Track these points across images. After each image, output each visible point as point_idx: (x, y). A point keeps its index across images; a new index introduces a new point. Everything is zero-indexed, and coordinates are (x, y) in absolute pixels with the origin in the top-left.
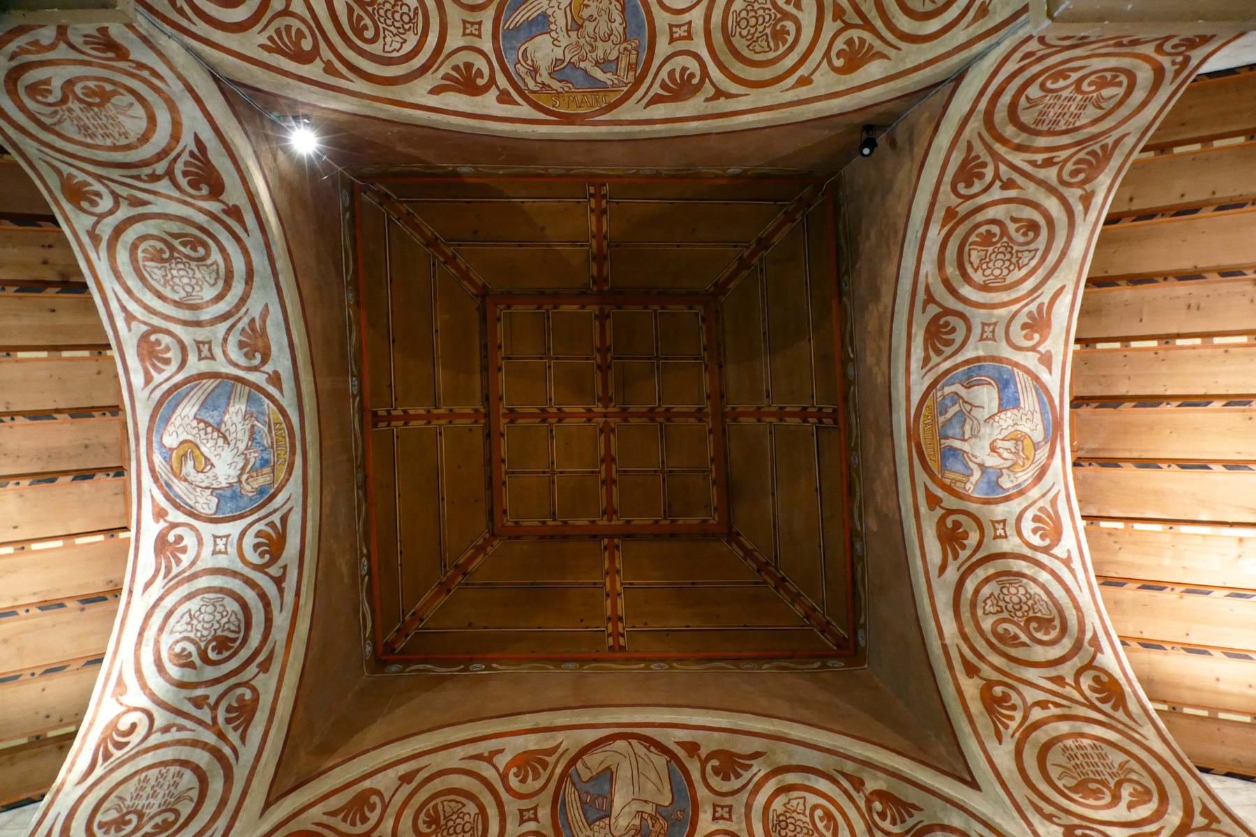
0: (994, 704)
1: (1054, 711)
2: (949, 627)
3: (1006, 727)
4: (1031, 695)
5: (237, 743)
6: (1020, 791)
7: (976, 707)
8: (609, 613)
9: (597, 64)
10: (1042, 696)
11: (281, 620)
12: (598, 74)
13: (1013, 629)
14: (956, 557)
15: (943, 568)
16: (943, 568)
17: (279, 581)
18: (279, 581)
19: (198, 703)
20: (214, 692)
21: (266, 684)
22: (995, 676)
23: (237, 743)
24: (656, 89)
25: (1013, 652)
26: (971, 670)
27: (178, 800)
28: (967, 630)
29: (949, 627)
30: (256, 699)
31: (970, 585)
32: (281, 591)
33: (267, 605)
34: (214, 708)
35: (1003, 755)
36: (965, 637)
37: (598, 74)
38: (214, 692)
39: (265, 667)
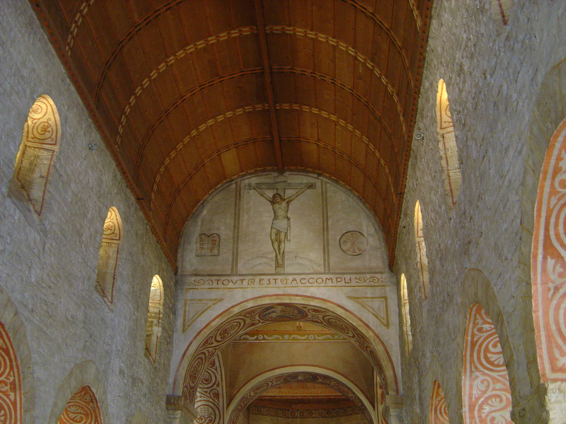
7: (379, 396)
11: (219, 377)
17: (216, 370)
18: (216, 370)
19: (206, 392)
20: (208, 390)
21: (219, 389)
30: (218, 393)
33: (214, 373)
34: (210, 393)
35: (381, 408)
38: (208, 390)
39: (218, 385)
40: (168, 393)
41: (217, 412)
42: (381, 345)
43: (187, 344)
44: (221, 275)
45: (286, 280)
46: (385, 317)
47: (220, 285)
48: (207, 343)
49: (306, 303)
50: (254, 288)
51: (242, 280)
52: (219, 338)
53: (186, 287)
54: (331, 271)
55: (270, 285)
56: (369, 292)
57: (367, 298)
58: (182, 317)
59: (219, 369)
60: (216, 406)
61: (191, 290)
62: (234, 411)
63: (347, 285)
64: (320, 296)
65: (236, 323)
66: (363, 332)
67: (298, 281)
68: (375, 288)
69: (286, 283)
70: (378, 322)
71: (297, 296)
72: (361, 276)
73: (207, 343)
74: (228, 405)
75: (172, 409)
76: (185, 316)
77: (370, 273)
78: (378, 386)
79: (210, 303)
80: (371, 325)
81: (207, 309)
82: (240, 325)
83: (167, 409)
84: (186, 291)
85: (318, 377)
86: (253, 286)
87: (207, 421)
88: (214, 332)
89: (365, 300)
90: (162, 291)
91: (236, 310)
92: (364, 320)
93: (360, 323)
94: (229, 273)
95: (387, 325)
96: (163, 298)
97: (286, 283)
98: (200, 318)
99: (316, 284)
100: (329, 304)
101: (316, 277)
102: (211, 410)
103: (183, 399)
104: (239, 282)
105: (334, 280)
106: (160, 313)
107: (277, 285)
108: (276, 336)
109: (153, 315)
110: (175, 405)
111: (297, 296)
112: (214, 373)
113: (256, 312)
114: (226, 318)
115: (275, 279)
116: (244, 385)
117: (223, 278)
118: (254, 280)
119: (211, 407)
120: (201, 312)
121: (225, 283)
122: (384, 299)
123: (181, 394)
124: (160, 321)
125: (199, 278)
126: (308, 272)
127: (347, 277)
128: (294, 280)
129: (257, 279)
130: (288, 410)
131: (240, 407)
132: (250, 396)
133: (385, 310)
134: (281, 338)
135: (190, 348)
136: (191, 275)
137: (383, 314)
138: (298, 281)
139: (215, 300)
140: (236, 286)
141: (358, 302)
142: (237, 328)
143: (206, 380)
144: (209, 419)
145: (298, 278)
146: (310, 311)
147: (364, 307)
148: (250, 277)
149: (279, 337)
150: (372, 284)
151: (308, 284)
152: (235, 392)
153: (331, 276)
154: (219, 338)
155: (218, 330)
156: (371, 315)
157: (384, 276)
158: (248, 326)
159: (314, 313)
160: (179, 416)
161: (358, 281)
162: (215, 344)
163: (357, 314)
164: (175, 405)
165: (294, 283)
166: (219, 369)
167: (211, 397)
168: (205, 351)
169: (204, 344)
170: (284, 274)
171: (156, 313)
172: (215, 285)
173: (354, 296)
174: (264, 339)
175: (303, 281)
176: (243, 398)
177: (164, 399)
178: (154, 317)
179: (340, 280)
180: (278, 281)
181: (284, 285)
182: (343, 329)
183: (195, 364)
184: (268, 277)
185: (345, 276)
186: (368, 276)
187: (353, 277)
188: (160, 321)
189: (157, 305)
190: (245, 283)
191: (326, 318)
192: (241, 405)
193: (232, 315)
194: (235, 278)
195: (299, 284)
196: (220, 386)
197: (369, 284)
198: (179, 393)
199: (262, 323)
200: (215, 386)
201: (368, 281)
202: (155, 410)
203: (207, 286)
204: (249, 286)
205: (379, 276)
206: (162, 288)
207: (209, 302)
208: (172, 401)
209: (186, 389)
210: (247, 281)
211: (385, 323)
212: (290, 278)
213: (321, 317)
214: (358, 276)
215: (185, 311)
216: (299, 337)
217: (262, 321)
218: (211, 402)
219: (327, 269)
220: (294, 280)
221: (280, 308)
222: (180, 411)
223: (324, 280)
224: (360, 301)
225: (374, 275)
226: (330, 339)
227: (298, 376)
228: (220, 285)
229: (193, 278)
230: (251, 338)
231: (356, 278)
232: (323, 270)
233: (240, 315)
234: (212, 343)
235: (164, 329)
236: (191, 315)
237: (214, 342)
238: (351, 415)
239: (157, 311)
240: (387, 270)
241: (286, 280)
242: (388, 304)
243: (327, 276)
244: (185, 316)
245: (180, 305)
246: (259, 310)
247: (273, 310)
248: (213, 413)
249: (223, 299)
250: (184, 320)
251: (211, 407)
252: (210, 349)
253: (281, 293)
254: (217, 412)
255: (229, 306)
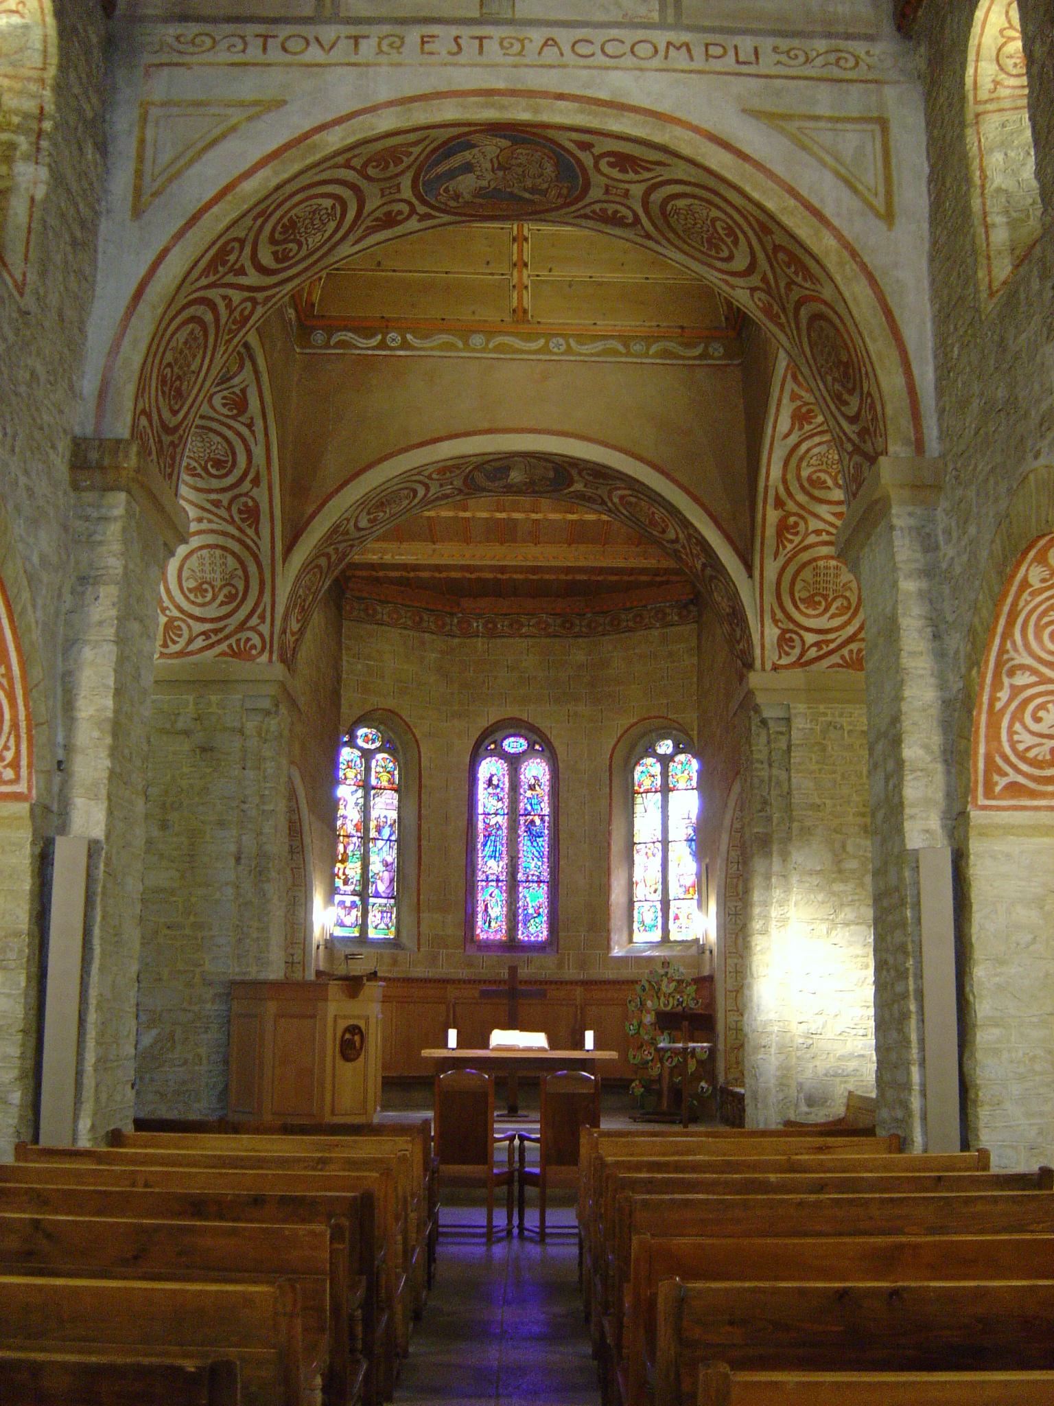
0: (783, 528)
1: (825, 537)
2: (776, 472)
3: (784, 547)
4: (814, 524)
5: (255, 538)
6: (770, 598)
7: (770, 531)
8: (515, 258)
9: (525, 190)
10: (821, 526)
11: (258, 451)
12: (527, 195)
13: (823, 476)
14: (801, 428)
15: (787, 436)
16: (787, 436)
17: (250, 426)
18: (250, 426)
19: (217, 504)
20: (225, 498)
21: (261, 494)
22: (794, 509)
23: (255, 538)
24: (588, 211)
25: (816, 493)
26: (779, 504)
27: (232, 577)
28: (789, 477)
29: (776, 472)
30: (257, 506)
31: (804, 447)
32: (253, 432)
33: (244, 440)
34: (229, 509)
35: (771, 569)
36: (784, 481)
37: (527, 195)
38: (225, 498)
39: (256, 482)
40: (78, 431)
41: (252, 568)
42: (864, 281)
43: (150, 256)
44: (275, 21)
45: (521, 41)
46: (881, 189)
47: (275, 54)
48: (224, 263)
49: (595, 123)
50: (400, 65)
51: (356, 39)
52: (266, 259)
53: (147, 58)
54: (686, 21)
55: (462, 59)
56: (824, 100)
57: (817, 118)
58: (132, 166)
59: (259, 423)
60: (248, 548)
61: (166, 70)
62: (306, 568)
63: (744, 69)
64: (646, 104)
65: (328, 203)
66: (803, 233)
67: (567, 49)
68: (844, 86)
69: (520, 54)
70: (856, 204)
71: (561, 97)
72: (796, 42)
73: (224, 263)
74: (288, 550)
75: (92, 488)
76: (141, 158)
77: (829, 35)
78: (771, 500)
79: (236, 116)
80: (828, 212)
81: (224, 136)
82: (344, 214)
83: (76, 487)
84: (147, 74)
85: (574, 472)
86: (395, 57)
87: (221, 598)
88: (248, 221)
89: (812, 124)
90: (52, 32)
91: (335, 140)
92: (804, 192)
93: (792, 202)
94: (308, 11)
95: (889, 217)
96: (54, 60)
97: (520, 54)
98: (197, 168)
99: (629, 61)
100: (678, 131)
101: (630, 36)
102: (231, 561)
103: (134, 449)
104: (344, 45)
105: (698, 51)
106: (41, 115)
107: (484, 60)
108: (445, 338)
109: (16, 120)
110: (102, 469)
111: (561, 97)
112: (244, 440)
113: (407, 161)
114: (297, 167)
115: (481, 39)
116: (337, 490)
117: (284, 31)
118: (402, 39)
119: (234, 554)
120: (200, 145)
121: (290, 45)
122: (877, 128)
123: (127, 436)
124: (44, 144)
125: (193, 29)
126: (600, 17)
127: (746, 44)
128: (549, 42)
129: (413, 35)
130: (452, 615)
131: (323, 561)
132: (359, 529)
133: (880, 164)
134: (460, 344)
135: (161, 271)
136: (168, 19)
137: (871, 177)
138: (567, 49)
139: (256, 103)
140: (336, 55)
141: (782, 131)
142: (332, 225)
143: (218, 464)
144: (225, 591)
145: (565, 37)
146: (603, 164)
147: (804, 148)
148: (386, 29)
149: (451, 339)
150: (836, 72)
151: (601, 59)
152: (310, 510)
153: (685, 37)
154: (266, 259)
155: (265, 215)
156: (828, 177)
157: (878, 49)
158: (368, 223)
159: (615, 173)
160: (119, 511)
161: (784, 58)
162: (253, 278)
163: (779, 170)
164: (102, 469)
165: (550, 54)
166: (259, 423)
167: (233, 522)
168: (213, 294)
169: (212, 267)
170: (512, 22)
171: (26, 116)
172: (254, 53)
173: (769, 107)
174: (405, 345)
175: (582, 49)
176: (335, 529)
177: (64, 445)
178: (18, 129)
179: (719, 51)
180: (492, 47)
181: (510, 60)
182: (713, 242)
183: (182, 336)
184: (454, 31)
185: (738, 40)
186: (821, 45)
187: (766, 44)
188: (44, 144)
189: (33, 87)
190: (367, 48)
191: (658, 196)
192: (328, 556)
193: (318, 157)
194: (329, 32)
195: (569, 56)
196: (264, 485)
197: (825, 72)
198: (121, 428)
199: (424, 217)
200: (247, 485)
201: (819, 61)
202: (27, 473)
203: (223, 57)
204: (383, 59)
205: (859, 48)
206: (50, 20)
207: (230, 111)
208: (94, 456)
209: (144, 421)
210: (373, 41)
211: (882, 210)
212: (537, 36)
213: (637, 190)
214: (784, 44)
215: (142, 142)
216: (518, 344)
217: (422, 209)
218: (233, 537)
219: (670, 11)
220: (549, 42)
221: (492, 147)
222: (122, 496)
223: (662, 48)
224: (792, 126)
225: (841, 44)
226: (616, 353)
227: (509, 469)
228: (275, 54)
229: (172, 30)
230: (361, 342)
231: (775, 49)
232: (655, 16)
233: (347, 165)
234: (242, 272)
235: (57, 179)
236: (166, 156)
237: (251, 271)
238: (631, 630)
239: (30, 106)
240: (888, 27)
241: (521, 41)
242: (892, 143)
243: (671, 36)
244: (141, 158)
245: (123, 122)
246: (416, 150)
247: (467, 155)
248: (240, 572)
249: (285, 102)
250: (139, 174)
251: (234, 554)
252: (236, 296)
253: (501, 85)
254: (252, 568)
255: (307, 126)
